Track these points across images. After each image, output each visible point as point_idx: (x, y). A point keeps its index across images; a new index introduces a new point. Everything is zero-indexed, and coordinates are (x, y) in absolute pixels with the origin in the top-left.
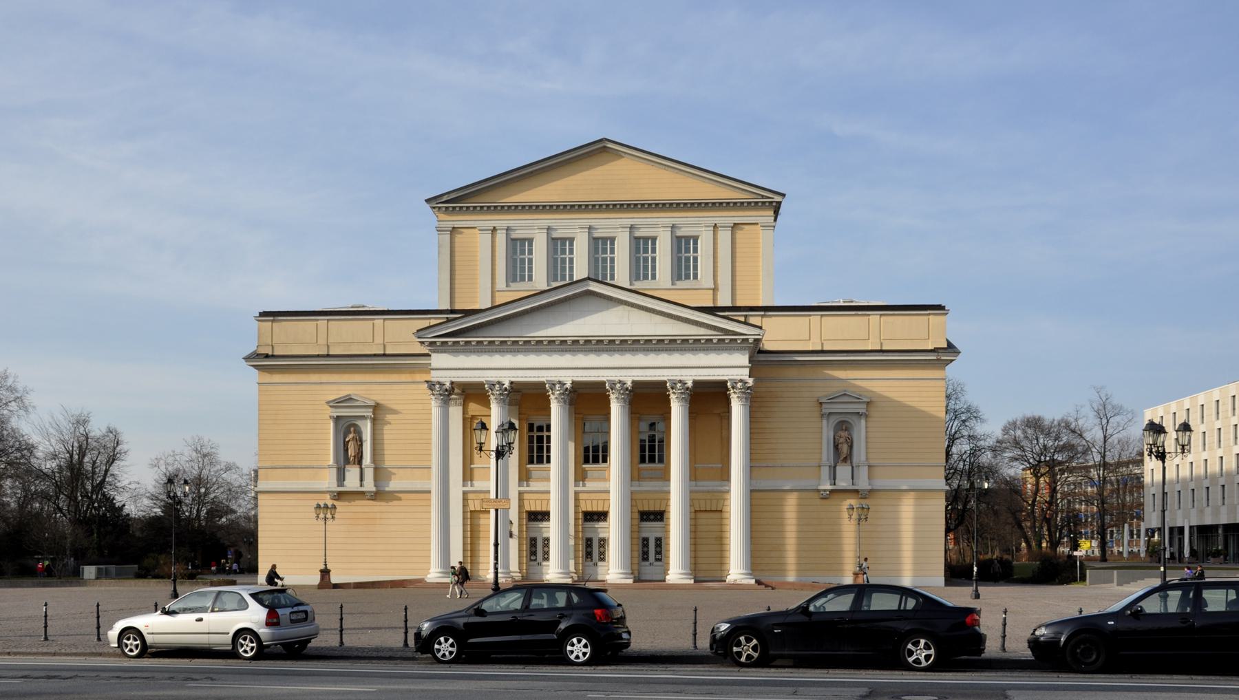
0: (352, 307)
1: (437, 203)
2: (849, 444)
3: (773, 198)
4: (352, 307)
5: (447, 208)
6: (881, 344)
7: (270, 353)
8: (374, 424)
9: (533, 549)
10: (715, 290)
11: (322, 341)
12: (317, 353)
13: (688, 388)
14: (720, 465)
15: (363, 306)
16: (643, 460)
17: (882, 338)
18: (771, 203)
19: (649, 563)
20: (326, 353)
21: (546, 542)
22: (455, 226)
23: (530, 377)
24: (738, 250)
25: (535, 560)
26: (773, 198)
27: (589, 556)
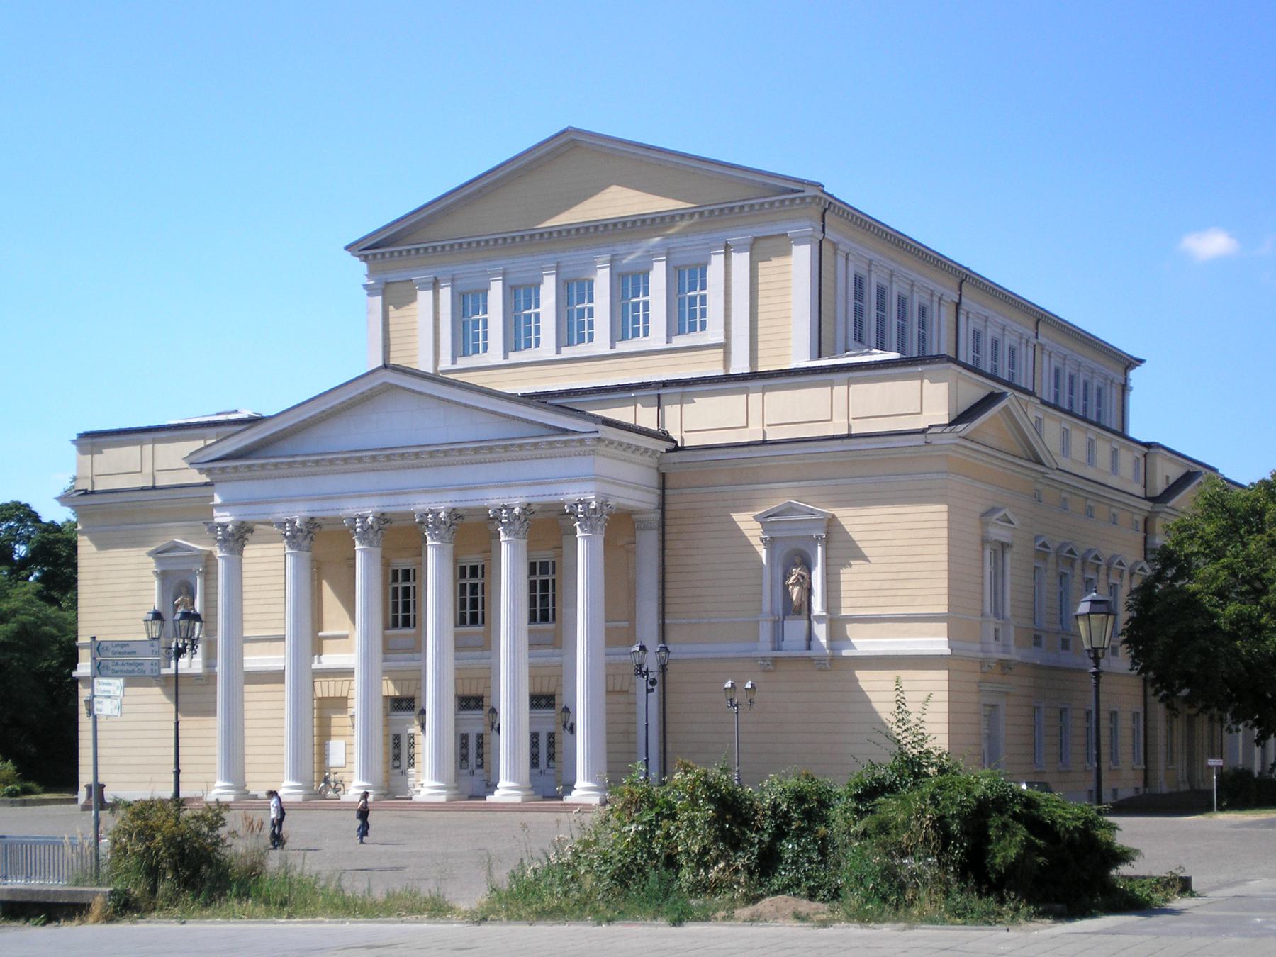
0: (218, 414)
1: (360, 250)
2: (806, 586)
3: (803, 191)
4: (218, 414)
5: (375, 255)
6: (849, 427)
7: (90, 489)
8: (205, 580)
9: (397, 751)
10: (725, 347)
11: (148, 469)
12: (141, 486)
13: (371, 527)
14: (626, 624)
15: (236, 411)
16: (395, 625)
17: (850, 417)
18: (803, 199)
19: (539, 770)
20: (151, 484)
21: (396, 741)
22: (389, 281)
23: (404, 505)
24: (760, 280)
25: (398, 767)
26: (803, 191)
27: (464, 761)
